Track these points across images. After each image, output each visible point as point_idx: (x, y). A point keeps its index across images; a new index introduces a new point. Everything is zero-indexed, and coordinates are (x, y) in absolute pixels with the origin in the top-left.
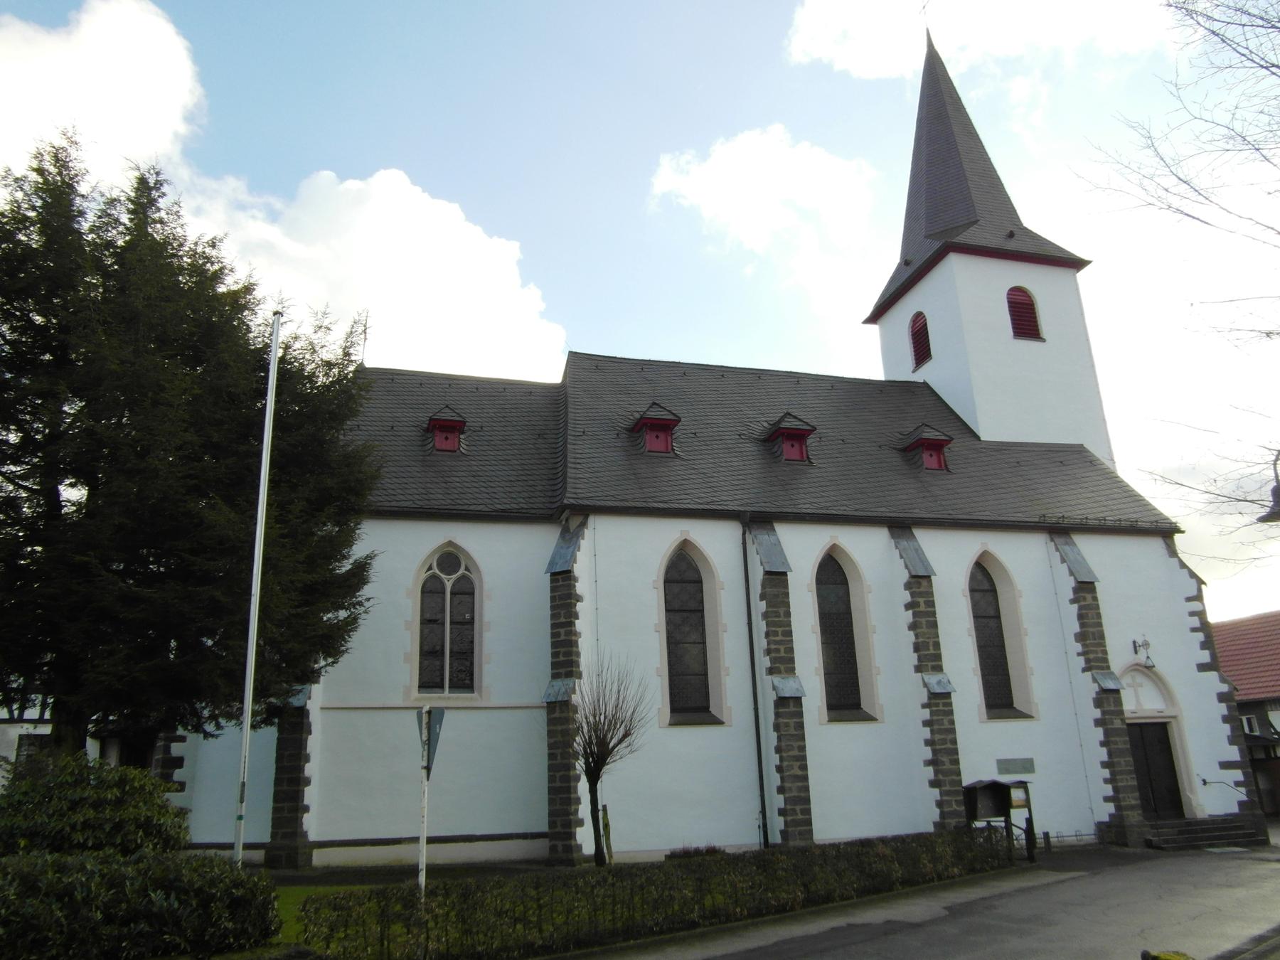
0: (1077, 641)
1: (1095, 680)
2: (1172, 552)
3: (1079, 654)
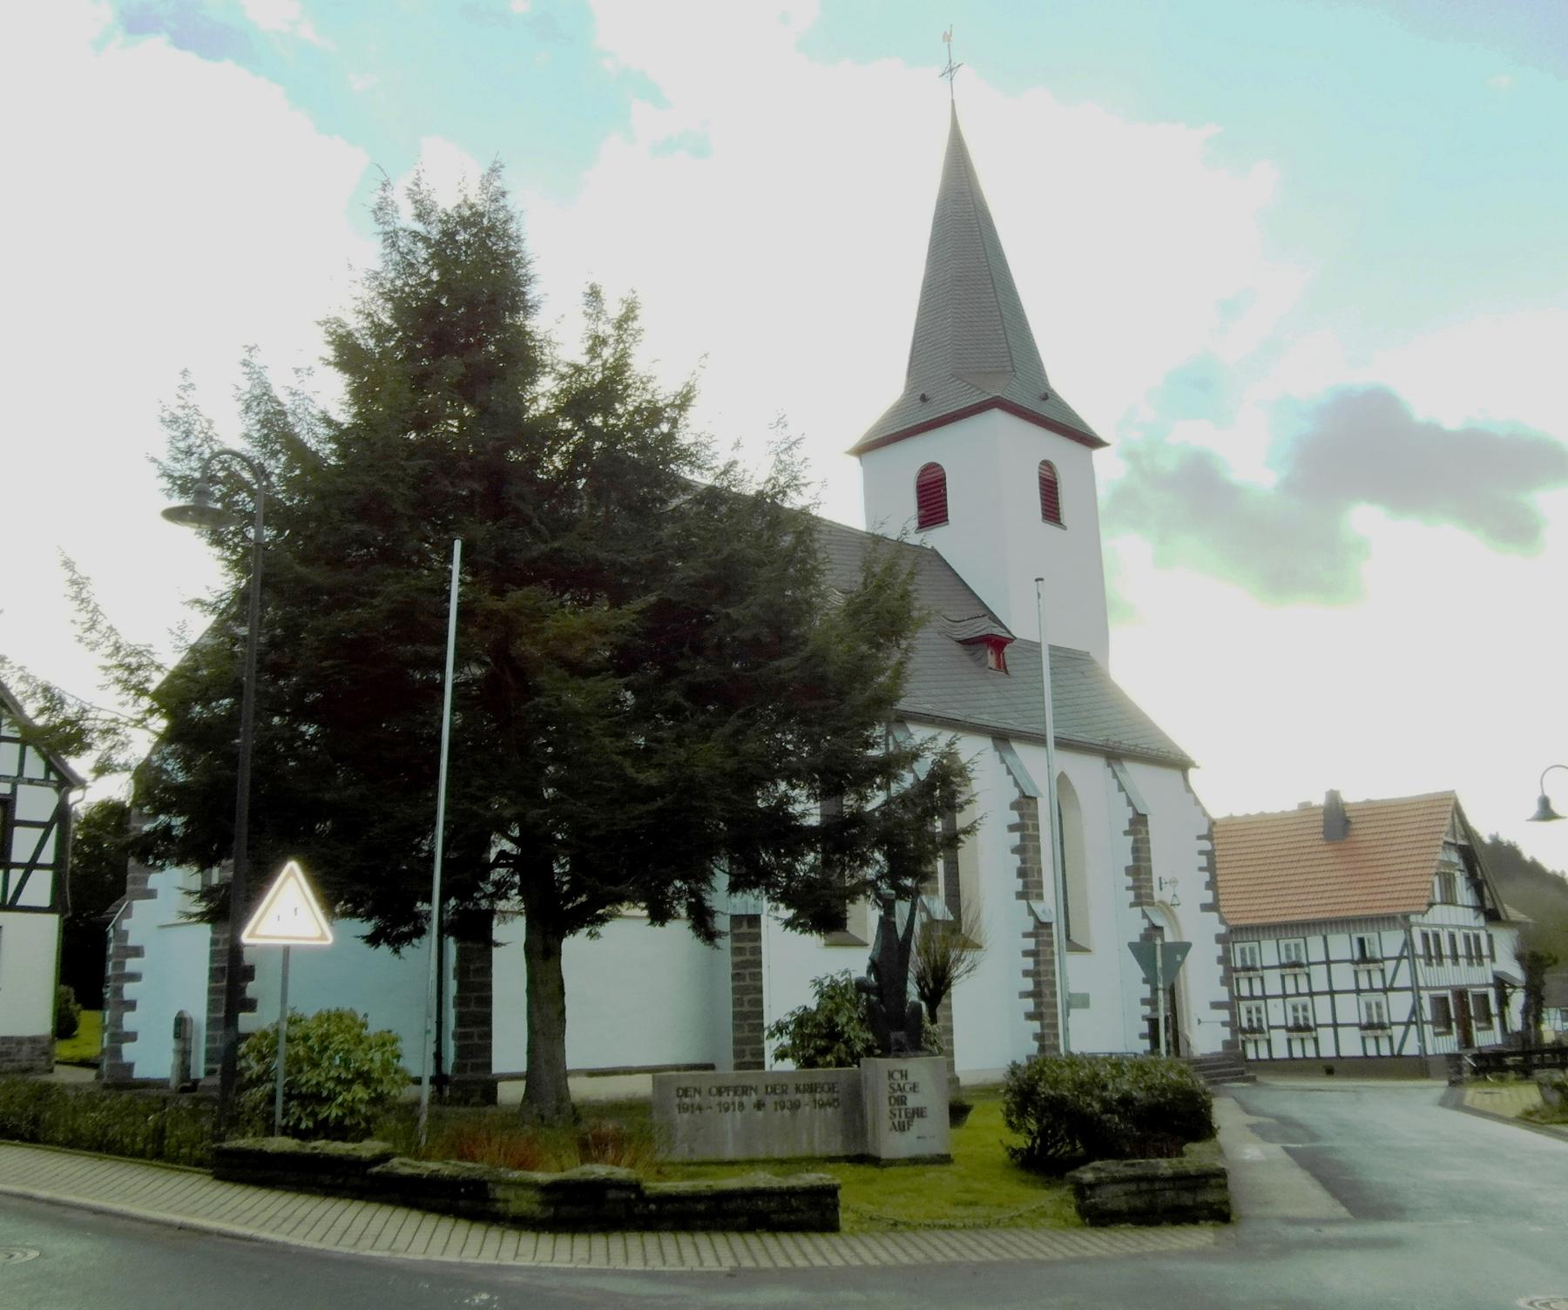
0: (1127, 874)
1: (1145, 916)
2: (1186, 779)
3: (1128, 888)
